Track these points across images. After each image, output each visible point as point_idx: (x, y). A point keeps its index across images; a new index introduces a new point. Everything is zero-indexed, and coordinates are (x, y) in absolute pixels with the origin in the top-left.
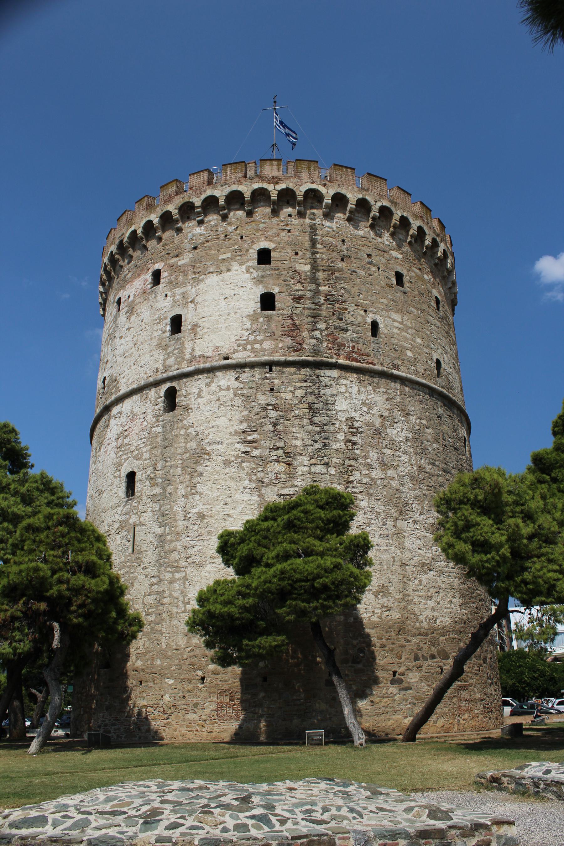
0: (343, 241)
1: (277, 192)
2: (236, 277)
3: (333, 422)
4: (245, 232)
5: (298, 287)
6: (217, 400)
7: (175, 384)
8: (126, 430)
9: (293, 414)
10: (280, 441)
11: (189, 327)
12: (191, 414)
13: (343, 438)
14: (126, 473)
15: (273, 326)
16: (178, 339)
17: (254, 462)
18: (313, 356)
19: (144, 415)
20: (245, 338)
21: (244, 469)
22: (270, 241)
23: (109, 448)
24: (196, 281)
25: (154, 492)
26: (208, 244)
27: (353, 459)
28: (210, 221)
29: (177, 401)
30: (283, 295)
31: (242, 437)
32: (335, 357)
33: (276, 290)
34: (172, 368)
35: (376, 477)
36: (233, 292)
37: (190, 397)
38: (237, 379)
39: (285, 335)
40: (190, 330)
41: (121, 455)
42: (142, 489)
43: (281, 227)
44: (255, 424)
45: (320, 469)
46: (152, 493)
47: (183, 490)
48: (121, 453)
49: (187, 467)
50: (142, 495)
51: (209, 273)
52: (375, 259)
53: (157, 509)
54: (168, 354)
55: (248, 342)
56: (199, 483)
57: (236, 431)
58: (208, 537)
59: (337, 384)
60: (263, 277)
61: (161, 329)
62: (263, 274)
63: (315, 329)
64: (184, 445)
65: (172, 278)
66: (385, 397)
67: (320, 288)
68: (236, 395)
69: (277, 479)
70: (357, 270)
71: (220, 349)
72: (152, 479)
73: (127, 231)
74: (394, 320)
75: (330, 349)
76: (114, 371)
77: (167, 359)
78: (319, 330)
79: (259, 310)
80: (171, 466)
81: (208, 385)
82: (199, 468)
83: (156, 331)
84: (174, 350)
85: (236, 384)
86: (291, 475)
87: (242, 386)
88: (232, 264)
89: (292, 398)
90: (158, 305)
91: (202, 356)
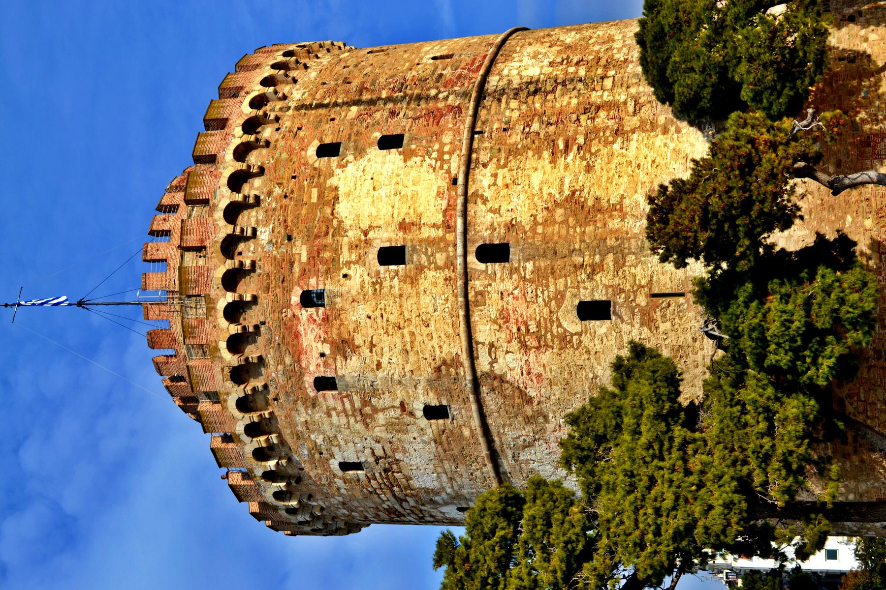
0: (324, 84)
1: (246, 136)
2: (348, 179)
7: (472, 249)
8: (519, 329)
9: (539, 108)
10: (570, 117)
11: (401, 234)
12: (519, 219)
14: (578, 320)
15: (425, 134)
16: (414, 249)
17: (591, 141)
18: (471, 97)
19: (505, 294)
20: (433, 162)
21: (599, 150)
22: (308, 146)
23: (537, 369)
24: (340, 230)
25: (611, 264)
26: (289, 219)
27: (599, 59)
28: (257, 221)
29: (497, 242)
30: (385, 128)
31: (559, 155)
32: (473, 80)
33: (378, 135)
34: (451, 254)
37: (496, 225)
38: (485, 165)
39: (438, 123)
40: (405, 233)
41: (552, 334)
42: (604, 285)
43: (291, 137)
44: (546, 143)
45: (608, 83)
46: (612, 267)
48: (549, 336)
49: (586, 218)
51: (332, 214)
52: (351, 62)
53: (633, 257)
54: (430, 264)
55: (440, 158)
56: (608, 201)
57: (550, 162)
59: (508, 76)
60: (356, 148)
61: (392, 279)
62: (352, 149)
64: (557, 226)
66: (527, 46)
68: (505, 166)
69: (614, 118)
70: (365, 72)
71: (441, 190)
72: (594, 270)
73: (221, 358)
74: (432, 49)
75: (463, 85)
76: (427, 372)
77: (436, 263)
78: (437, 95)
79: (401, 149)
81: (485, 201)
82: (590, 203)
83: (391, 287)
84: (426, 254)
85: (491, 167)
86: (609, 106)
87: (495, 160)
88: (328, 186)
89: (519, 110)
90: (354, 292)
91: (445, 212)
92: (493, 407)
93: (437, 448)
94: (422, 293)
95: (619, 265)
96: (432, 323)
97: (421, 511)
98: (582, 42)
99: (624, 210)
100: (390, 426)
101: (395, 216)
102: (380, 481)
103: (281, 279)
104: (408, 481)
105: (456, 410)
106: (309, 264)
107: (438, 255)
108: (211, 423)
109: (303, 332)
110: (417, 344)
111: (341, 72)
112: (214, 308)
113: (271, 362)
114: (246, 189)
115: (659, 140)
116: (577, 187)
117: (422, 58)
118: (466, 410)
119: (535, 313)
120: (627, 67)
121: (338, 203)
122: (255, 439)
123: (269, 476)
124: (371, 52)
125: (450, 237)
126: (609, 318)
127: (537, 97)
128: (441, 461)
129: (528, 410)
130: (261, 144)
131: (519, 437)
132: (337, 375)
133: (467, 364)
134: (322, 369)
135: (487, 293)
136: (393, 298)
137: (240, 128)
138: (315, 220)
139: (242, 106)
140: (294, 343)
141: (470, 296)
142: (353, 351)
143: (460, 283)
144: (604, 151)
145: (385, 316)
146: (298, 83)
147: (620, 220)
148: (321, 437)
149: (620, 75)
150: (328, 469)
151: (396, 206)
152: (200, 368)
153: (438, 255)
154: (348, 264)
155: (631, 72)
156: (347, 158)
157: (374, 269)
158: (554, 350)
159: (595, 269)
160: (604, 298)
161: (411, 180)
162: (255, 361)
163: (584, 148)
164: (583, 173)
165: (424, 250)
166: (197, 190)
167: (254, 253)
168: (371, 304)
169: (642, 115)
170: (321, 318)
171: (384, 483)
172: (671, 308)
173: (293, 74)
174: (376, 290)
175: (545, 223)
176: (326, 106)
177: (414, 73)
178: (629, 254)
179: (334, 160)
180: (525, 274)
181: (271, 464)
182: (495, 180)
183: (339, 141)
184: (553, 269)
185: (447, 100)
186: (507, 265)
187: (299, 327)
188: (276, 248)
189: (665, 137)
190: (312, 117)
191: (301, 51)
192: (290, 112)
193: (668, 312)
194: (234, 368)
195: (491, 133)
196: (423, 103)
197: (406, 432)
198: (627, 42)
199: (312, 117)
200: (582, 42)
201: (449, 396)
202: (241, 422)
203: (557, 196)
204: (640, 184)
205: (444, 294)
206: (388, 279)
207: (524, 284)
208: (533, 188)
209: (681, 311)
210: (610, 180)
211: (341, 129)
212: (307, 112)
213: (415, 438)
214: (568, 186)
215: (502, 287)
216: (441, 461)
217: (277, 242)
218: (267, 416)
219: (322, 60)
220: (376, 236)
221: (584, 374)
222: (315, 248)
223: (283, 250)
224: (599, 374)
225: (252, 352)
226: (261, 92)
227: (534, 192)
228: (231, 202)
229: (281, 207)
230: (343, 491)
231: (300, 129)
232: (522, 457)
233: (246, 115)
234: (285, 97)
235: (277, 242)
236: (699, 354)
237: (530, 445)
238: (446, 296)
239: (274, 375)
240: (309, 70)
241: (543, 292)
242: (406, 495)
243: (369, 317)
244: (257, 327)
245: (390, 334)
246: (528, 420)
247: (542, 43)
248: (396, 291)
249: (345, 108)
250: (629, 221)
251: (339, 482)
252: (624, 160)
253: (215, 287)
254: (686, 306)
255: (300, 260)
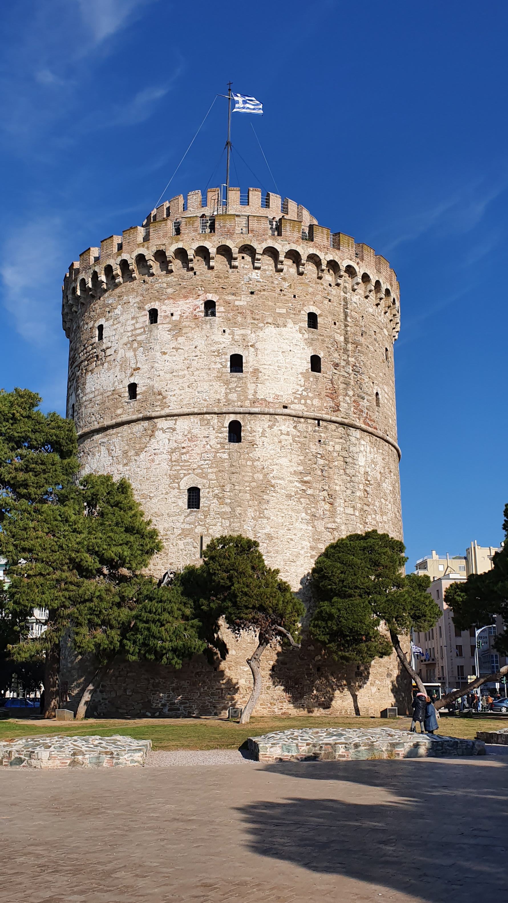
1: (326, 262)
2: (291, 334)
3: (357, 474)
4: (297, 292)
5: (336, 355)
6: (279, 442)
8: (184, 448)
13: (362, 488)
16: (241, 379)
17: (308, 499)
18: (346, 418)
19: (207, 439)
20: (300, 393)
24: (256, 328)
25: (223, 510)
26: (265, 293)
27: (368, 505)
28: (265, 270)
29: (242, 434)
30: (326, 360)
31: (300, 477)
32: (358, 420)
34: (236, 404)
35: (379, 520)
36: (289, 348)
37: (255, 434)
38: (295, 427)
39: (328, 396)
40: (252, 372)
43: (324, 295)
44: (309, 468)
45: (350, 511)
47: (252, 513)
49: (255, 494)
50: (209, 509)
51: (267, 323)
52: (379, 337)
53: (228, 525)
54: (230, 389)
55: (302, 397)
56: (267, 509)
57: (295, 471)
58: (276, 555)
61: (221, 363)
62: (312, 337)
63: (346, 395)
64: (251, 475)
65: (230, 315)
66: (382, 457)
67: (350, 359)
68: (294, 441)
70: (370, 346)
71: (280, 398)
72: (220, 498)
74: (386, 393)
76: (158, 386)
78: (349, 396)
79: (310, 370)
80: (240, 491)
81: (271, 427)
82: (265, 497)
84: (236, 387)
85: (294, 432)
86: (333, 513)
88: (287, 320)
90: (213, 337)
92: (134, 429)
93: (110, 391)
94: (211, 384)
95: (222, 515)
96: (191, 390)
97: (73, 380)
98: (382, 494)
99: (260, 519)
100: (125, 360)
101: (263, 366)
102: (91, 352)
103: (224, 287)
104: (91, 371)
105: (133, 405)
106: (234, 307)
107: (235, 395)
108: (129, 236)
109: (187, 301)
110: (177, 379)
111: (371, 329)
112: (205, 239)
113: (169, 279)
114: (289, 262)
115: (306, 544)
116: (276, 488)
117: (378, 385)
118: (133, 412)
119: (194, 459)
120: (361, 524)
121: (275, 327)
122: (118, 266)
123: (95, 275)
124: (387, 350)
125: (247, 403)
126: (189, 507)
127: (342, 463)
128: (102, 394)
129: (132, 453)
130: (320, 273)
131: (115, 446)
132: (159, 324)
133: (163, 413)
134: (163, 314)
135: (208, 427)
136: (208, 364)
137: (332, 259)
138: (264, 311)
139: (348, 260)
140: (181, 295)
141: (207, 415)
142: (174, 336)
143: (216, 410)
144: (301, 507)
145: (196, 358)
146: (365, 299)
147: (253, 516)
148: (119, 313)
149: (355, 519)
150: (99, 316)
151: (270, 367)
152: (165, 229)
153: (235, 395)
154: (232, 334)
155: (357, 526)
156: (306, 333)
157: (228, 352)
158: (169, 471)
159: (220, 499)
160: (201, 505)
161: (288, 377)
162: (169, 268)
163: (303, 494)
164: (286, 493)
165: (239, 385)
166: (288, 228)
167: (243, 267)
168: (204, 349)
169: (326, 533)
170: (197, 315)
171: (90, 355)
172: (193, 548)
173: (372, 295)
174: (214, 352)
175: (253, 466)
176: (346, 320)
177: (367, 380)
178: (230, 522)
179: (306, 325)
180: (220, 453)
181: (103, 278)
182: (284, 434)
183: (319, 328)
184: (222, 471)
185: (344, 403)
186: (227, 441)
187: (192, 299)
188: (246, 284)
189: (309, 548)
190: (338, 309)
191: (390, 301)
192: (342, 294)
193: (190, 547)
194: (165, 252)
195: (318, 431)
196: (342, 386)
197: (121, 370)
198: (380, 524)
199: (338, 309)
200: (382, 494)
201: (142, 400)
202: (130, 257)
203: (272, 475)
204: (277, 530)
205: (209, 398)
206: (221, 361)
207: (213, 452)
208: (278, 459)
209: (190, 555)
210: (280, 510)
211: (327, 330)
212: (342, 305)
213: (116, 376)
214: (278, 482)
215: (211, 437)
216: (102, 394)
217: (250, 284)
218: (133, 275)
219: (382, 316)
220: (251, 352)
221: (152, 491)
222: (244, 311)
223: (244, 288)
224: (152, 500)
225: (176, 265)
226: (358, 273)
227: (274, 460)
228: (278, 252)
229: (274, 287)
230: (86, 326)
231: (330, 301)
232: (102, 448)
233: (341, 263)
234: (354, 290)
235: (250, 284)
236: (162, 566)
237: (110, 454)
238: (208, 400)
239: (160, 280)
240: (375, 307)
241: (207, 464)
242: (82, 370)
243: (196, 348)
244: (192, 269)
245: (184, 362)
246: (125, 453)
247: (384, 468)
248: (213, 366)
249: (343, 332)
250: (252, 523)
251: (91, 325)
252: (294, 520)
253: (220, 240)
254: (194, 559)
255: (237, 300)
